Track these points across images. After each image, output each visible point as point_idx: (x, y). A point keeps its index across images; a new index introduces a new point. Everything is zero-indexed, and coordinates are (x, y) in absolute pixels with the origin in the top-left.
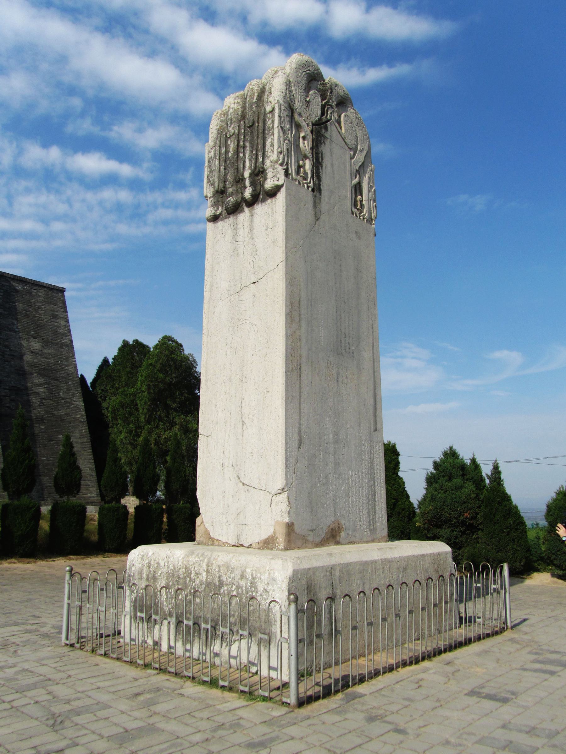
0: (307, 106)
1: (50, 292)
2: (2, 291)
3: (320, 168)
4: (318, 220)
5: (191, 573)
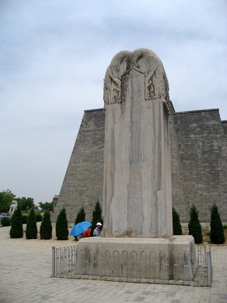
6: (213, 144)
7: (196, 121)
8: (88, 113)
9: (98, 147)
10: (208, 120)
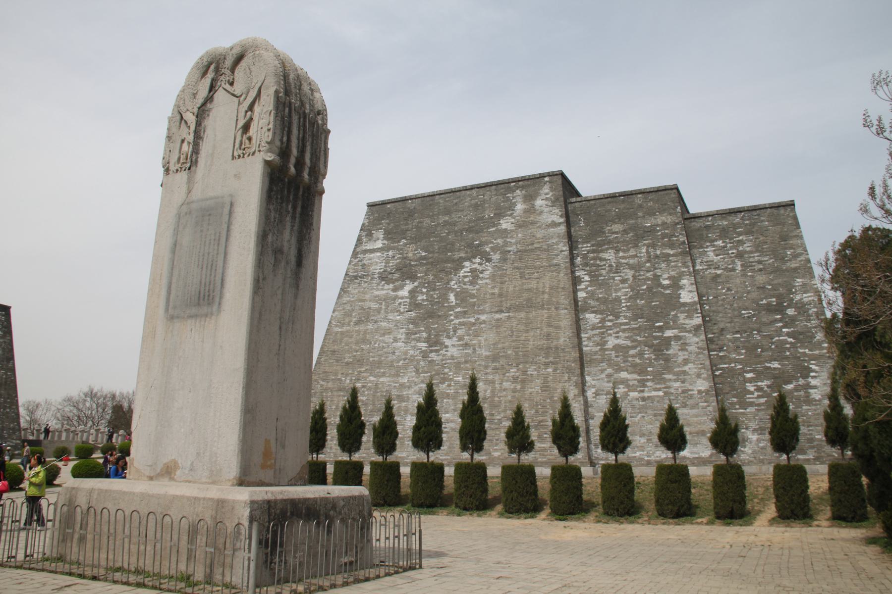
1: (775, 211)
2: (718, 231)
3: (201, 142)
6: (658, 272)
7: (620, 217)
8: (374, 208)
9: (391, 286)
10: (651, 213)
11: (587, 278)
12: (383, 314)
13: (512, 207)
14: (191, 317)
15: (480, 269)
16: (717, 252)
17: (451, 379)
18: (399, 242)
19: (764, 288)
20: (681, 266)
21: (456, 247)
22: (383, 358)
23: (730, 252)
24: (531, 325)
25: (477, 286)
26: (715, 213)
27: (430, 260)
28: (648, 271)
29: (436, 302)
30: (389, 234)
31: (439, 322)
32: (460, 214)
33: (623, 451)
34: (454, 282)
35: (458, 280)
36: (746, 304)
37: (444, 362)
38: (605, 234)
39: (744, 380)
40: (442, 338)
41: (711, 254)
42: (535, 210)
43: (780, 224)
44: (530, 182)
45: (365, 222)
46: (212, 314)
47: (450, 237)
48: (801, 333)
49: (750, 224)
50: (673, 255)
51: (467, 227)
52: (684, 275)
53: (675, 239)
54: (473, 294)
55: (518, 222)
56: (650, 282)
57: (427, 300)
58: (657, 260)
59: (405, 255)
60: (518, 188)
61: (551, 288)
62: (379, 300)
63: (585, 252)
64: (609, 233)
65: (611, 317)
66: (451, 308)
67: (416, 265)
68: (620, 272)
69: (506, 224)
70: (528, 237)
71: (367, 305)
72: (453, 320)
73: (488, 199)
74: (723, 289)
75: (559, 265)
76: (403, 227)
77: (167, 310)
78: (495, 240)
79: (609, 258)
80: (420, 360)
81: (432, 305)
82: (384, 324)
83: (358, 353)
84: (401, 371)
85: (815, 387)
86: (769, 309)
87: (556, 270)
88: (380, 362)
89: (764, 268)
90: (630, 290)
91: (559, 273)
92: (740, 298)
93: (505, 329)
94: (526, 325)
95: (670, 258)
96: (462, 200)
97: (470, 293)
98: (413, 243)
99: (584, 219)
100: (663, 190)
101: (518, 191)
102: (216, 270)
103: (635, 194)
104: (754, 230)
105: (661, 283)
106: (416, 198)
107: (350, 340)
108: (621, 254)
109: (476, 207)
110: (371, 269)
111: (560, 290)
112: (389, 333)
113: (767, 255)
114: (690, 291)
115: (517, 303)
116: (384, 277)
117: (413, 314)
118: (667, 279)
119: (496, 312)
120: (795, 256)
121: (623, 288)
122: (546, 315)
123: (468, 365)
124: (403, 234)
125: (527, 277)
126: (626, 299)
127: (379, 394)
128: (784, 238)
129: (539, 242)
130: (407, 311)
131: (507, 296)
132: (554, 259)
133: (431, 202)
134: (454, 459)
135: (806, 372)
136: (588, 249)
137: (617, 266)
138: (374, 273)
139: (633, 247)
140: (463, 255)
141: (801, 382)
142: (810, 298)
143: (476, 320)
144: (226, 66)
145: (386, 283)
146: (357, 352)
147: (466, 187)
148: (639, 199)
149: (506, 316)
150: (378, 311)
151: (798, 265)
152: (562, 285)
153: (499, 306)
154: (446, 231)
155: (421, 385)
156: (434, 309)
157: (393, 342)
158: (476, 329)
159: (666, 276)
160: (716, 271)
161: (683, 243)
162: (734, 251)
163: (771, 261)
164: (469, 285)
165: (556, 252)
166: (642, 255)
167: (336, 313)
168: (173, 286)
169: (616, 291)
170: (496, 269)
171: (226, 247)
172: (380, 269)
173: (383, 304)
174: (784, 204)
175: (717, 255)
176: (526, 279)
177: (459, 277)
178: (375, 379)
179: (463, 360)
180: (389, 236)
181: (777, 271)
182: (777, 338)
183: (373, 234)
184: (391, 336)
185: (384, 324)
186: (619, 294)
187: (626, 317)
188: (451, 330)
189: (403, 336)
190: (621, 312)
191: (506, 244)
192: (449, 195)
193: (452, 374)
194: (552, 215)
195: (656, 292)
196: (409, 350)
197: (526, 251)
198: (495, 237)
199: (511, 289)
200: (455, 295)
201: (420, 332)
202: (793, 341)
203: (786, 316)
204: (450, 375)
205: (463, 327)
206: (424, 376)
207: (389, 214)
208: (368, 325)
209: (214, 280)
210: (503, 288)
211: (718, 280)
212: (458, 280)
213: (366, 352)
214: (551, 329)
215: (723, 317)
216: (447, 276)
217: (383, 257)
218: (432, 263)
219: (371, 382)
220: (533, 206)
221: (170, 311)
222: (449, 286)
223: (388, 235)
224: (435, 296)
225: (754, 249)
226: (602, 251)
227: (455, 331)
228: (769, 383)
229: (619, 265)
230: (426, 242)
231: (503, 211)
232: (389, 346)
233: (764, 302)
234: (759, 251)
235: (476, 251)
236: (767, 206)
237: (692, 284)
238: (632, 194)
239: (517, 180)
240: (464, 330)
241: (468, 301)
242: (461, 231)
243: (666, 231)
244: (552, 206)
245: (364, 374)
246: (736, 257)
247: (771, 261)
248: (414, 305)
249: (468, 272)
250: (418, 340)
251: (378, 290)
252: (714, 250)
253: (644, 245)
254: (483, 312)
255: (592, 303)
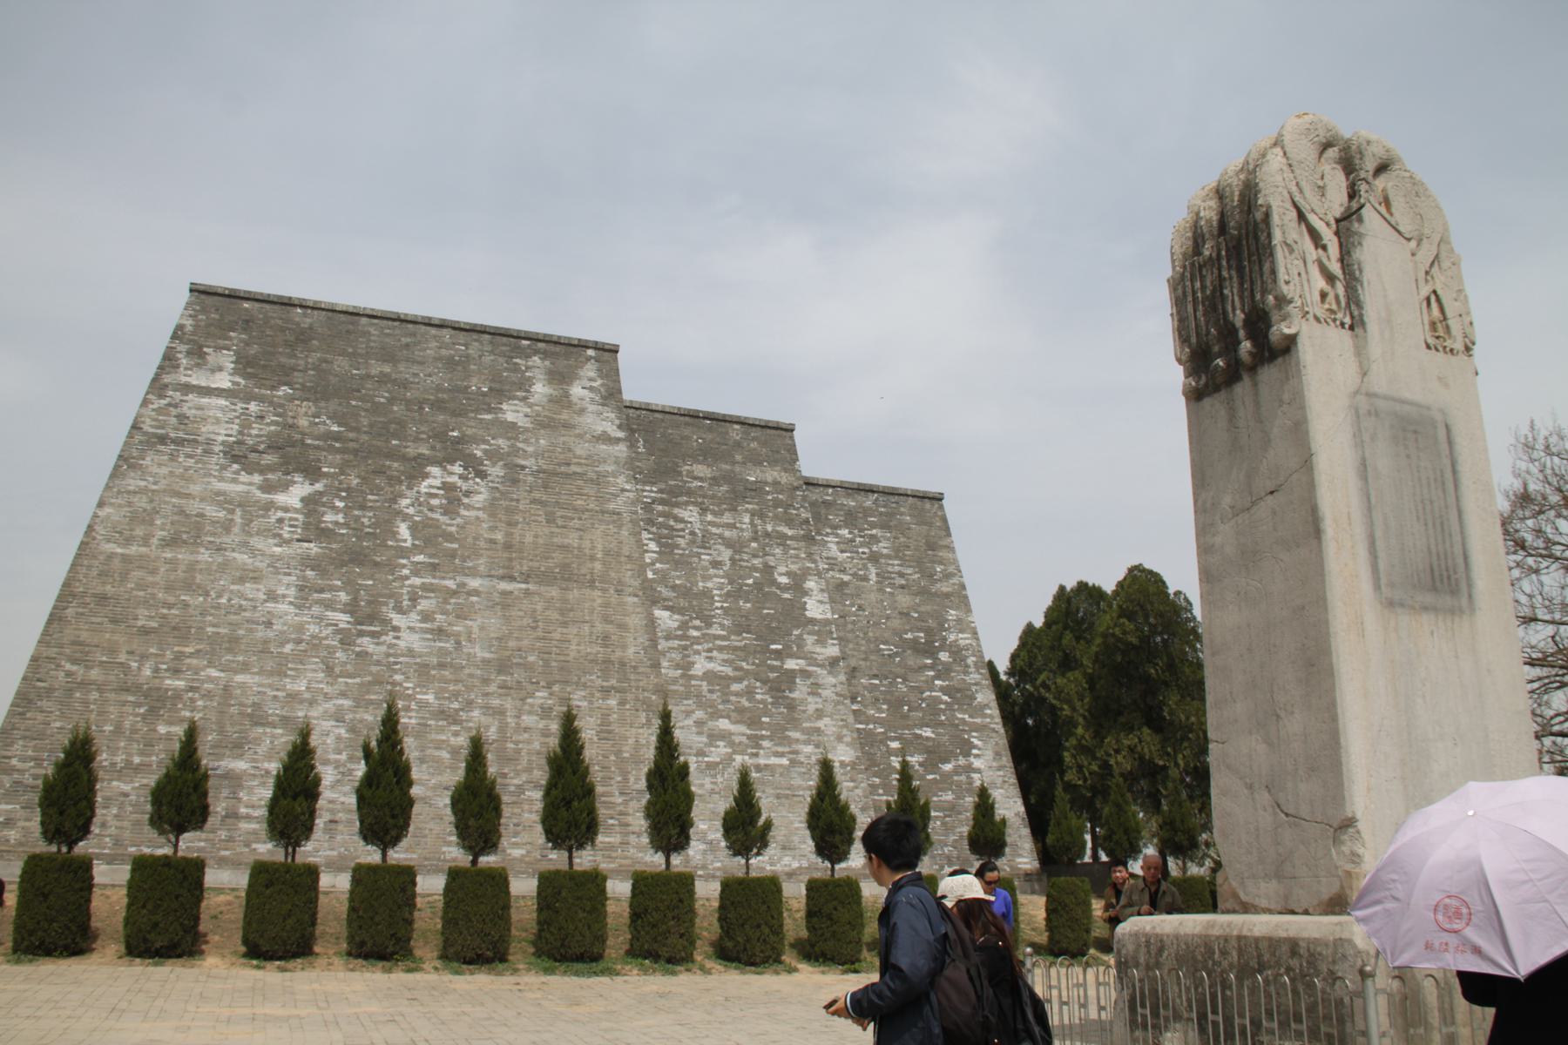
0: (1323, 195)
1: (918, 503)
2: (842, 513)
3: (1359, 287)
4: (1365, 374)
5: (1214, 953)
6: (771, 561)
7: (706, 454)
8: (210, 300)
9: (257, 478)
11: (653, 546)
12: (235, 536)
13: (525, 384)
14: (1425, 609)
15: (464, 488)
16: (843, 547)
17: (410, 696)
18: (273, 388)
19: (907, 614)
20: (804, 559)
21: (410, 432)
22: (241, 632)
23: (860, 550)
24: (571, 614)
25: (459, 520)
26: (839, 484)
27: (352, 445)
28: (755, 556)
29: (368, 533)
30: (249, 364)
31: (377, 576)
32: (415, 369)
33: (395, 841)
34: (408, 501)
35: (417, 499)
36: (886, 635)
37: (392, 659)
38: (682, 476)
39: (887, 751)
40: (384, 609)
41: (834, 547)
42: (570, 405)
43: (926, 524)
44: (558, 349)
45: (185, 322)
46: (1462, 611)
47: (395, 408)
48: (958, 690)
49: (886, 514)
50: (791, 538)
51: (432, 397)
52: (810, 574)
53: (795, 512)
54: (451, 534)
55: (537, 415)
56: (758, 575)
57: (346, 525)
58: (767, 541)
59: (290, 421)
60: (536, 352)
61: (607, 553)
62: (230, 503)
63: (649, 500)
64: (687, 476)
65: (697, 623)
66: (403, 552)
67: (317, 448)
68: (710, 548)
69: (513, 413)
70: (559, 450)
71: (194, 507)
72: (407, 578)
73: (476, 356)
74: (852, 605)
75: (619, 514)
76: (283, 360)
77: (1377, 587)
78: (493, 439)
79: (690, 520)
80: (335, 646)
81: (359, 538)
82: (242, 558)
83: (173, 611)
84: (290, 665)
85: (978, 771)
86: (915, 646)
87: (614, 522)
88: (234, 640)
89: (907, 585)
90: (726, 581)
91: (620, 527)
92: (877, 624)
93: (521, 614)
94: (562, 612)
95: (788, 542)
96: (420, 342)
97: (444, 530)
98: (308, 400)
99: (644, 441)
100: (774, 428)
101: (536, 358)
102: (1451, 535)
103: (730, 422)
104: (892, 524)
105: (776, 579)
106: (316, 307)
107: (151, 579)
108: (710, 517)
109: (450, 364)
110: (203, 429)
111: (623, 559)
112: (255, 580)
113: (910, 567)
114: (821, 602)
115: (543, 569)
116: (238, 455)
117: (313, 548)
118: (784, 574)
119: (502, 578)
120: (947, 576)
121: (716, 576)
122: (599, 601)
123: (447, 673)
124: (285, 375)
125: (560, 523)
126: (720, 596)
127: (234, 710)
128: (932, 546)
129: (579, 464)
130: (298, 540)
131: (521, 551)
132: (609, 500)
133: (351, 327)
134: (426, 859)
135: (966, 751)
136: (653, 495)
137: (703, 536)
138: (210, 442)
139: (729, 510)
140: (427, 452)
141: (962, 761)
142: (968, 642)
143: (458, 585)
144: (1367, 169)
145: (243, 469)
146: (169, 608)
147: (430, 318)
148: (735, 432)
149: (521, 589)
150: (227, 527)
151: (950, 589)
152: (626, 551)
153: (503, 567)
154: (386, 395)
155: (340, 702)
156: (362, 547)
157: (266, 601)
158: (459, 604)
159: (782, 569)
160: (842, 576)
161: (807, 521)
162: (866, 550)
163: (917, 576)
164: (442, 514)
165: (612, 490)
166: (744, 526)
167: (107, 510)
168: (1380, 544)
169: (706, 578)
170: (497, 495)
171: (1457, 499)
172: (226, 435)
173: (238, 512)
174: (931, 496)
175: (842, 552)
176: (558, 527)
177: (418, 492)
178: (222, 675)
179: (435, 660)
180: (249, 370)
181: (923, 592)
182: (928, 693)
183: (206, 353)
184: (261, 587)
185: (242, 558)
186: (710, 585)
187: (722, 626)
188: (406, 597)
189: (292, 592)
190: (714, 616)
191: (515, 451)
192: (390, 323)
193: (410, 685)
194: (603, 420)
195: (768, 593)
196: (309, 623)
197: (556, 474)
198: (492, 432)
199: (529, 539)
200: (409, 528)
201: (332, 589)
202: (949, 700)
203: (938, 662)
204: (408, 688)
205: (432, 595)
206: (346, 683)
207: (247, 322)
208: (198, 553)
209: (1453, 553)
210: (512, 534)
211: (846, 591)
212: (417, 499)
213: (197, 612)
214: (610, 628)
215: (854, 650)
216: (391, 486)
217: (235, 411)
218: (355, 452)
219: (210, 679)
220: (567, 395)
221: (1383, 587)
222: (397, 506)
223: (245, 365)
224: (365, 520)
225: (892, 553)
226: (677, 505)
227: (414, 599)
228: (921, 760)
229: (706, 535)
230: (340, 404)
231: (507, 387)
232: (255, 607)
233: (909, 636)
234: (901, 559)
235: (453, 451)
236: (909, 493)
237: (822, 590)
238: (725, 421)
239: (534, 338)
240: (434, 601)
241: (440, 544)
242: (421, 404)
243: (781, 497)
244: (603, 405)
245: (194, 661)
246: (868, 559)
247: (917, 576)
248: (315, 530)
249: (439, 488)
250: (329, 605)
251: (221, 479)
252: (838, 543)
253: (747, 510)
254: (474, 573)
255: (665, 592)
